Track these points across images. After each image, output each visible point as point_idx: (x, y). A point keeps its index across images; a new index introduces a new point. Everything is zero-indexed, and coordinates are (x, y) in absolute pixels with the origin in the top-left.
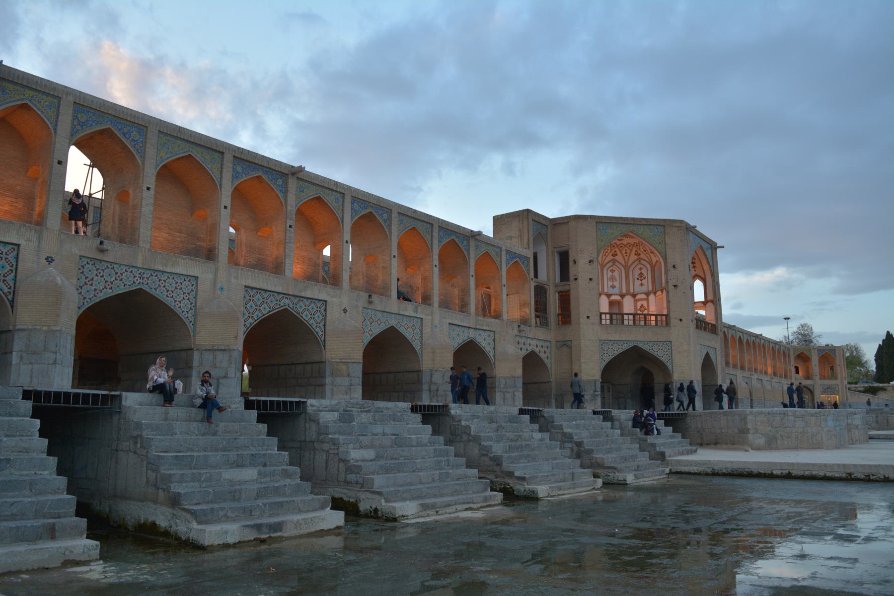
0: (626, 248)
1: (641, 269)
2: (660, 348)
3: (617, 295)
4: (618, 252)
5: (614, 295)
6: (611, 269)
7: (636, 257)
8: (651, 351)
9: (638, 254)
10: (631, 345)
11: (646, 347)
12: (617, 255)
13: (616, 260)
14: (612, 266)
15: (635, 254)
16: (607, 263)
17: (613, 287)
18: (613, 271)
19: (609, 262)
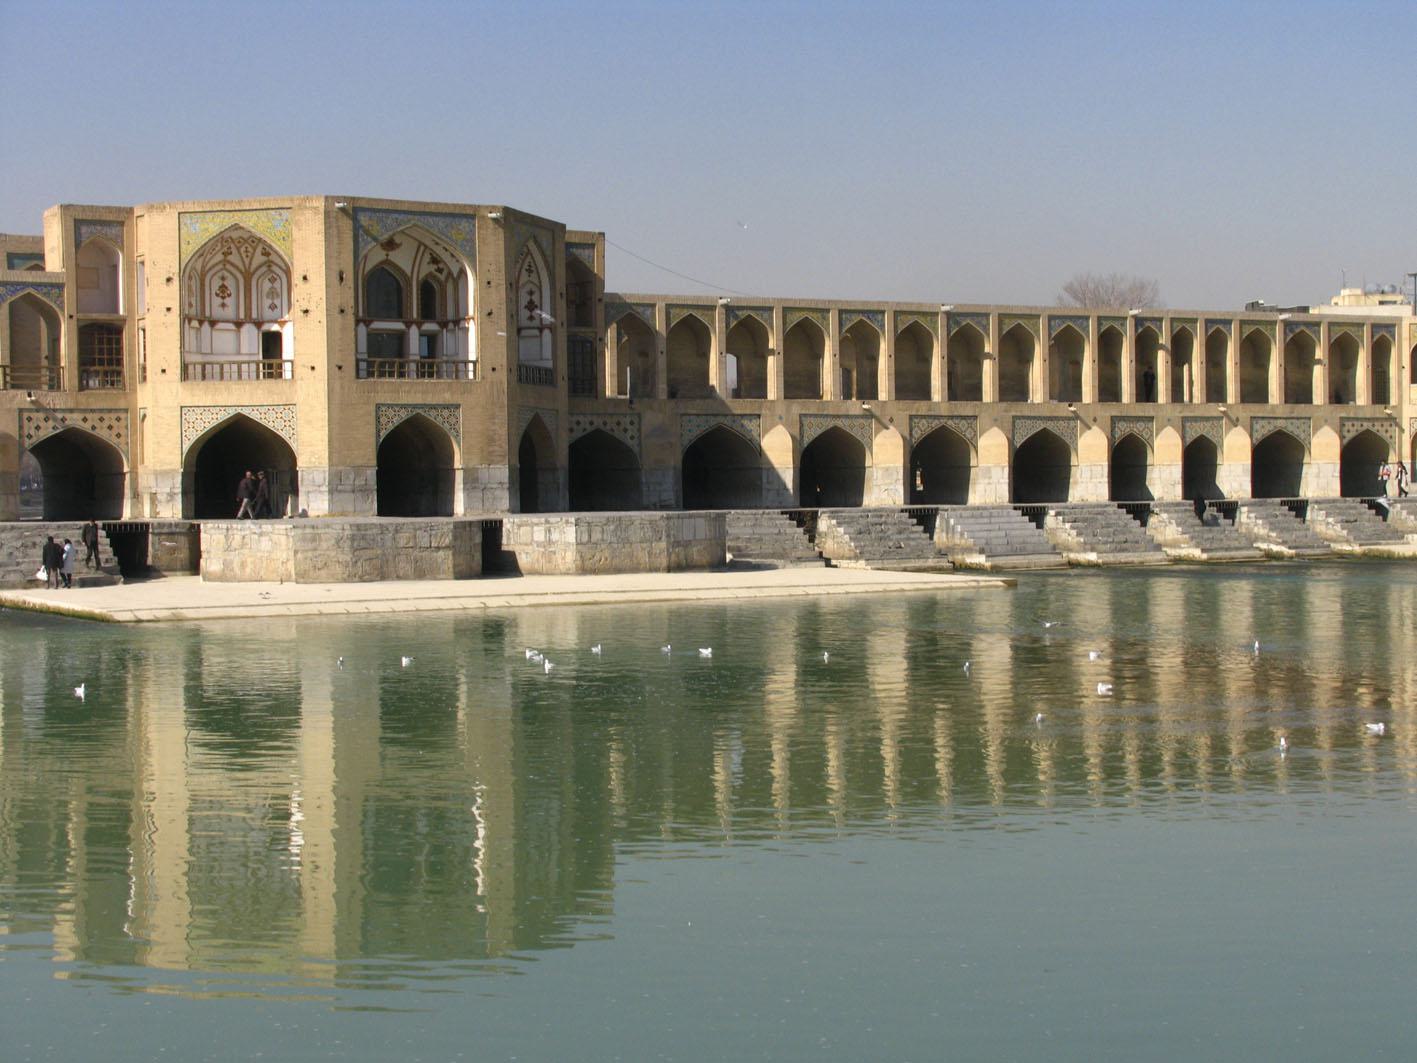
0: (247, 245)
1: (272, 280)
2: (279, 415)
3: (227, 321)
4: (234, 250)
5: (223, 322)
6: (220, 274)
7: (264, 258)
8: (263, 422)
9: (267, 254)
10: (232, 412)
11: (255, 415)
12: (231, 253)
13: (229, 262)
14: (222, 269)
15: (263, 254)
16: (213, 266)
17: (223, 305)
18: (223, 278)
19: (217, 264)
